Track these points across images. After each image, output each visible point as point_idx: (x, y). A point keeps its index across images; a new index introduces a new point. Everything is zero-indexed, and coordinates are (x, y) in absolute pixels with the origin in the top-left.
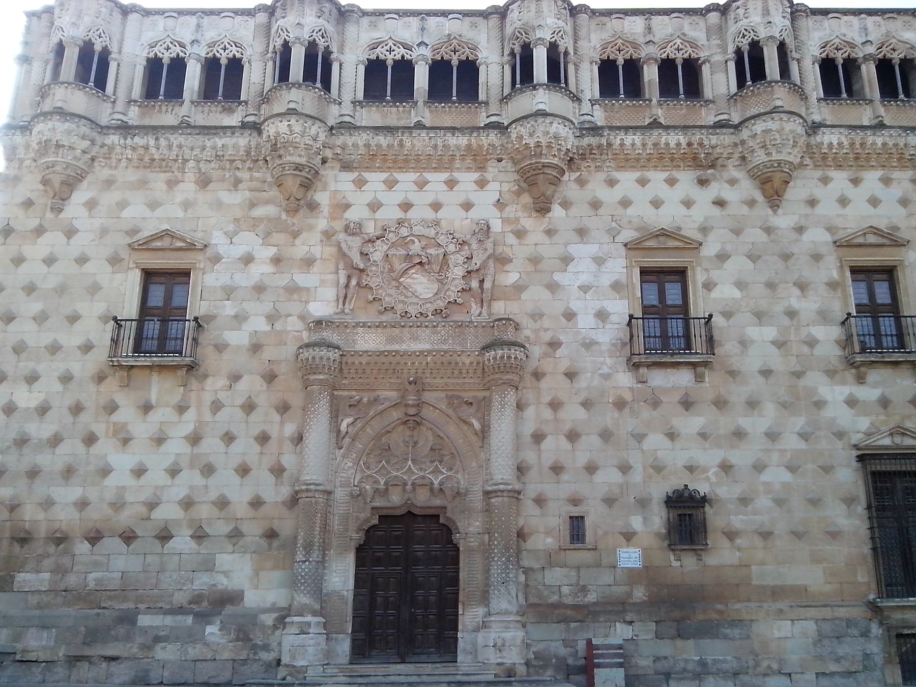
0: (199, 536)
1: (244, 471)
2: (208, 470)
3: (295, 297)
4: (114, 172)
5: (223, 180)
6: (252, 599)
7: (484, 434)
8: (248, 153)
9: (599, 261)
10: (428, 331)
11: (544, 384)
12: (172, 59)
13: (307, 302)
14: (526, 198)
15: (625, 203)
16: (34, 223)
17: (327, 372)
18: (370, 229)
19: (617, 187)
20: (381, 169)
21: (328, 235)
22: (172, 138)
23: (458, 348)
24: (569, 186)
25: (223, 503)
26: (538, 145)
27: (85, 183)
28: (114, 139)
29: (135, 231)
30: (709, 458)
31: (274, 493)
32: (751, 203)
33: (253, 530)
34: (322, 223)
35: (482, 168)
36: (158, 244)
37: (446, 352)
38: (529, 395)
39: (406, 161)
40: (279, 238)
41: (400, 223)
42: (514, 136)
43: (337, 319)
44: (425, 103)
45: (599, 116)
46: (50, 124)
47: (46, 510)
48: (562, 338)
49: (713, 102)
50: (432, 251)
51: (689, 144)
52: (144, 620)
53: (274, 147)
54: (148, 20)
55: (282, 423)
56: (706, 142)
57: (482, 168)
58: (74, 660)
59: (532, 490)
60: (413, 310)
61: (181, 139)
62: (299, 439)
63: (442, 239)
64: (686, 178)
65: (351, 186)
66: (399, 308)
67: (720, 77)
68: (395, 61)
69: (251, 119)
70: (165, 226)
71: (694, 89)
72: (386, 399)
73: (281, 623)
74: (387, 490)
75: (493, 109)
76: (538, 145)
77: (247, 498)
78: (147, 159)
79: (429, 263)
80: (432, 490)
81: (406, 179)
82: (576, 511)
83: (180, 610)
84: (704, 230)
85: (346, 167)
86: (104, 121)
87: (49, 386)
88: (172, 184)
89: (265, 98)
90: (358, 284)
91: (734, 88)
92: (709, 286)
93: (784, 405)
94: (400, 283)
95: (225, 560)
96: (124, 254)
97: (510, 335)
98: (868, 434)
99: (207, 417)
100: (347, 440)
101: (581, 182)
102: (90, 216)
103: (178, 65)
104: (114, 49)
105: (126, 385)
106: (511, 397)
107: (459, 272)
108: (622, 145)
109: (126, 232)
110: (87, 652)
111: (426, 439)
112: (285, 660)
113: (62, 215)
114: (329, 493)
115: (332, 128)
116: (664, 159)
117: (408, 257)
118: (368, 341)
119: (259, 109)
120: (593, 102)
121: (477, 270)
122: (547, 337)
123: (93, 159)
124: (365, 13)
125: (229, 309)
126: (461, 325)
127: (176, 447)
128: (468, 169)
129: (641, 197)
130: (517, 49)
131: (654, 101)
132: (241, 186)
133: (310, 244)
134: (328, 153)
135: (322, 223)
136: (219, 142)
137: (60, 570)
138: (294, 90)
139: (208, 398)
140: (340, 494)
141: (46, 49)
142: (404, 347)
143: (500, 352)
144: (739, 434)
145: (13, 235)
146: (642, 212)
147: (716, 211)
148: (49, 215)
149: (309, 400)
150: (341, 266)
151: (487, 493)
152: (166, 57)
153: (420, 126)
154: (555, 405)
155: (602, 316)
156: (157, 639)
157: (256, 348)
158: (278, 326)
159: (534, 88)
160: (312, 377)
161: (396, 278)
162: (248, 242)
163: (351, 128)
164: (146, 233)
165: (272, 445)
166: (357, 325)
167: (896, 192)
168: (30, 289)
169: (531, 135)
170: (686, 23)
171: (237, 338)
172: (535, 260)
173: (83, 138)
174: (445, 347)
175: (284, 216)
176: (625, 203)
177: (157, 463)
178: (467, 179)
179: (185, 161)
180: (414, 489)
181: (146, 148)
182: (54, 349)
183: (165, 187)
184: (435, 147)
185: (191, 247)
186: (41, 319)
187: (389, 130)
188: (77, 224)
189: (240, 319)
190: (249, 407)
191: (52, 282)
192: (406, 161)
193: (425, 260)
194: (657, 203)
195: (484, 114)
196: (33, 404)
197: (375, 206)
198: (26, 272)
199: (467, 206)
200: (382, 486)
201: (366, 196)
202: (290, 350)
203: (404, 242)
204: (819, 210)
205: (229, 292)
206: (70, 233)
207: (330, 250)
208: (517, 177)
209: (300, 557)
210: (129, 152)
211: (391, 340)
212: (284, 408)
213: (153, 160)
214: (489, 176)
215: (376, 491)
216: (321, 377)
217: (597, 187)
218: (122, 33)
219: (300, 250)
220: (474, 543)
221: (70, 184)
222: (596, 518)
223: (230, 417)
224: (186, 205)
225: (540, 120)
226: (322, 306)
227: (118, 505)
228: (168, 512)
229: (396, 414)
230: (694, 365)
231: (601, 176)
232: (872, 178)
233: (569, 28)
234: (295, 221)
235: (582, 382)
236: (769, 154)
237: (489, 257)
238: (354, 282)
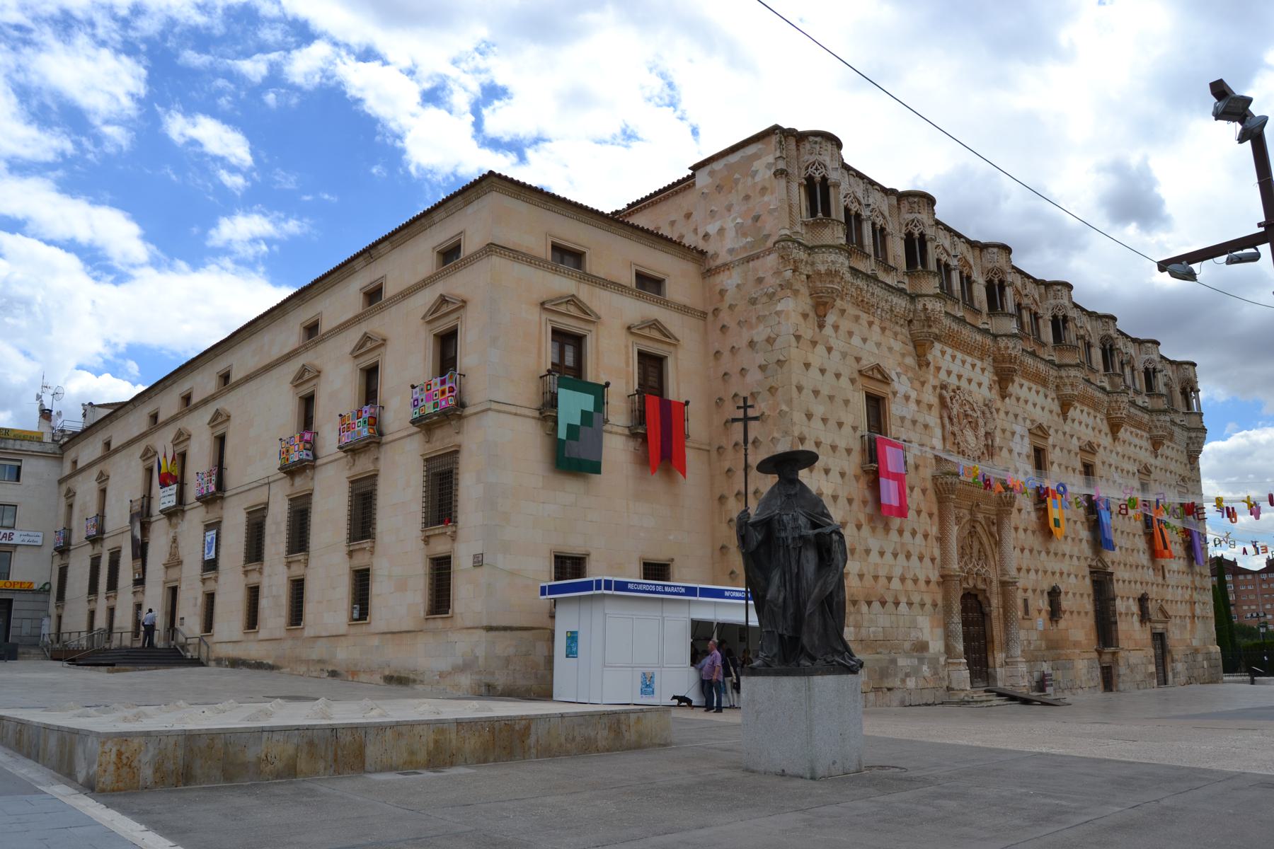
0: (910, 604)
7: (998, 543)
14: (997, 386)
21: (935, 388)
31: (935, 576)
33: (928, 600)
40: (917, 384)
41: (959, 388)
52: (902, 662)
57: (982, 359)
62: (942, 539)
83: (907, 654)
88: (871, 324)
92: (1052, 463)
96: (856, 375)
107: (982, 432)
112: (954, 685)
117: (966, 416)
130: (996, 281)
132: (899, 337)
135: (932, 381)
150: (945, 415)
151: (1004, 584)
156: (907, 675)
157: (917, 467)
212: (931, 515)
224: (878, 345)
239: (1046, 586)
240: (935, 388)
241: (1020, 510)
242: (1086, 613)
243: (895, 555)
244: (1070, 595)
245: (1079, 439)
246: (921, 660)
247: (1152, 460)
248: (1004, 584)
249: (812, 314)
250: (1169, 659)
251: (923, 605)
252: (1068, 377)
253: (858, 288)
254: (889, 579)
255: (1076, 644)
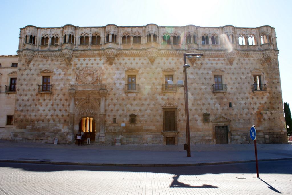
0: (54, 121)
1: (60, 110)
2: (55, 110)
3: (68, 81)
4: (37, 59)
5: (55, 60)
6: (63, 131)
7: (100, 104)
8: (59, 55)
9: (121, 74)
10: (90, 87)
11: (110, 96)
12: (46, 37)
13: (70, 82)
14: (108, 62)
15: (126, 63)
16: (24, 68)
17: (74, 94)
18: (81, 68)
19: (125, 60)
20: (83, 57)
21: (73, 70)
22: (46, 53)
23: (95, 90)
24: (116, 60)
25: (57, 116)
26: (109, 53)
27: (32, 61)
28: (37, 53)
29: (41, 69)
30: (137, 108)
32: (148, 63)
33: (62, 120)
34: (72, 67)
35: (100, 57)
36: (45, 72)
37: (93, 90)
38: (107, 98)
39: (87, 56)
40: (65, 70)
41: (86, 67)
42: (106, 51)
43: (75, 85)
44: (91, 45)
45: (122, 47)
46: (26, 51)
47: (30, 116)
48: (113, 88)
49: (142, 44)
50: (91, 72)
51: (137, 53)
52: (46, 134)
53: (64, 55)
54: (42, 30)
55: (66, 103)
56: (140, 52)
57: (100, 57)
58: (36, 139)
59: (107, 114)
60: (88, 83)
61: (48, 53)
62: (69, 105)
63: (93, 70)
64: (137, 59)
65: (77, 61)
66: (86, 82)
67: (144, 40)
68: (85, 37)
69: (60, 49)
70: (46, 68)
71: (140, 41)
72: (84, 98)
73: (67, 134)
74: (84, 114)
75: (103, 46)
76: (109, 53)
77: (61, 115)
78: (42, 56)
79: (91, 74)
80: (91, 114)
81: (87, 59)
82: (115, 117)
84: (139, 68)
85: (77, 57)
86: (35, 49)
87: (29, 96)
88: (47, 61)
89: (62, 45)
90: (79, 78)
91: (146, 42)
92: (140, 78)
93: (151, 100)
94: (86, 78)
95: (58, 124)
96: (39, 73)
97: (104, 88)
98: (165, 104)
99: (54, 101)
100: (77, 105)
101: (118, 59)
102: (34, 67)
103: (47, 38)
104: (36, 36)
105: (41, 96)
106: (104, 98)
108: (125, 53)
109: (40, 70)
110: (38, 138)
111: (90, 105)
112: (68, 140)
113: (29, 67)
114: (74, 114)
115: (74, 50)
116: (133, 55)
117: (87, 74)
118: (80, 89)
119: (61, 47)
120: (121, 45)
121: (99, 76)
122: (111, 87)
123: (33, 56)
124: (80, 28)
125: (57, 83)
126: (96, 86)
127: (50, 106)
128: (98, 57)
129: (129, 62)
131: (132, 44)
132: (59, 61)
133: (70, 71)
134: (73, 55)
135: (72, 67)
136: (54, 53)
137: (33, 126)
138: (67, 44)
139: (54, 98)
140: (76, 114)
141: (24, 36)
142: (86, 90)
143: (102, 91)
144: (143, 105)
145: (21, 70)
146: (129, 65)
147: (142, 65)
148: (27, 67)
149: (71, 99)
152: (45, 37)
153: (90, 50)
154: (112, 99)
155: (121, 84)
157: (62, 90)
158: (65, 86)
159: (109, 43)
160: (71, 95)
161: (85, 77)
162: (60, 71)
163: (77, 50)
164: (43, 70)
165: (65, 106)
166: (78, 86)
167: (174, 61)
168: (25, 80)
169: (108, 51)
170: (139, 30)
171: (59, 88)
172: (109, 74)
173: (32, 53)
174: (93, 90)
175: (66, 66)
176: (126, 63)
177: (47, 109)
178: (98, 59)
179: (49, 57)
180: (88, 114)
181: (42, 54)
182: (29, 90)
183: (46, 61)
184: (92, 53)
185: (50, 72)
186: (27, 85)
187: (84, 50)
188: (31, 68)
189: (59, 85)
190: (61, 100)
191: (28, 79)
192: (87, 56)
193: (90, 74)
194: (131, 63)
195: (101, 47)
196: (26, 99)
197: (82, 64)
198: (24, 77)
199: (98, 64)
200: (83, 113)
201: (80, 62)
202: (67, 90)
203: (86, 71)
204: (160, 65)
205: (57, 80)
206: (30, 70)
207: (74, 72)
208: (106, 58)
209: (70, 124)
210: (39, 55)
211: (84, 88)
212: (66, 100)
213: (43, 56)
214: (102, 58)
215: (82, 114)
216: (72, 95)
217: (121, 60)
218: (37, 32)
219: (69, 72)
220: (98, 122)
221: (30, 62)
222: (118, 118)
223: (58, 101)
224: (49, 65)
225: (110, 49)
226: (73, 82)
227: (41, 116)
228: (49, 117)
229: (85, 101)
230: (136, 93)
231: (122, 58)
232: (170, 59)
233: (117, 31)
234: (68, 67)
235: (117, 96)
236: (151, 55)
237: (101, 73)
238: (78, 78)
239: (129, 114)
240: (73, 70)
241: (115, 94)
242: (158, 121)
243: (49, 110)
244: (146, 116)
245: (162, 68)
246: (56, 134)
247: (228, 67)
248: (100, 115)
249: (25, 64)
250: (229, 135)
251: (60, 121)
252: (148, 52)
253: (40, 55)
254: (46, 116)
255: (147, 130)
